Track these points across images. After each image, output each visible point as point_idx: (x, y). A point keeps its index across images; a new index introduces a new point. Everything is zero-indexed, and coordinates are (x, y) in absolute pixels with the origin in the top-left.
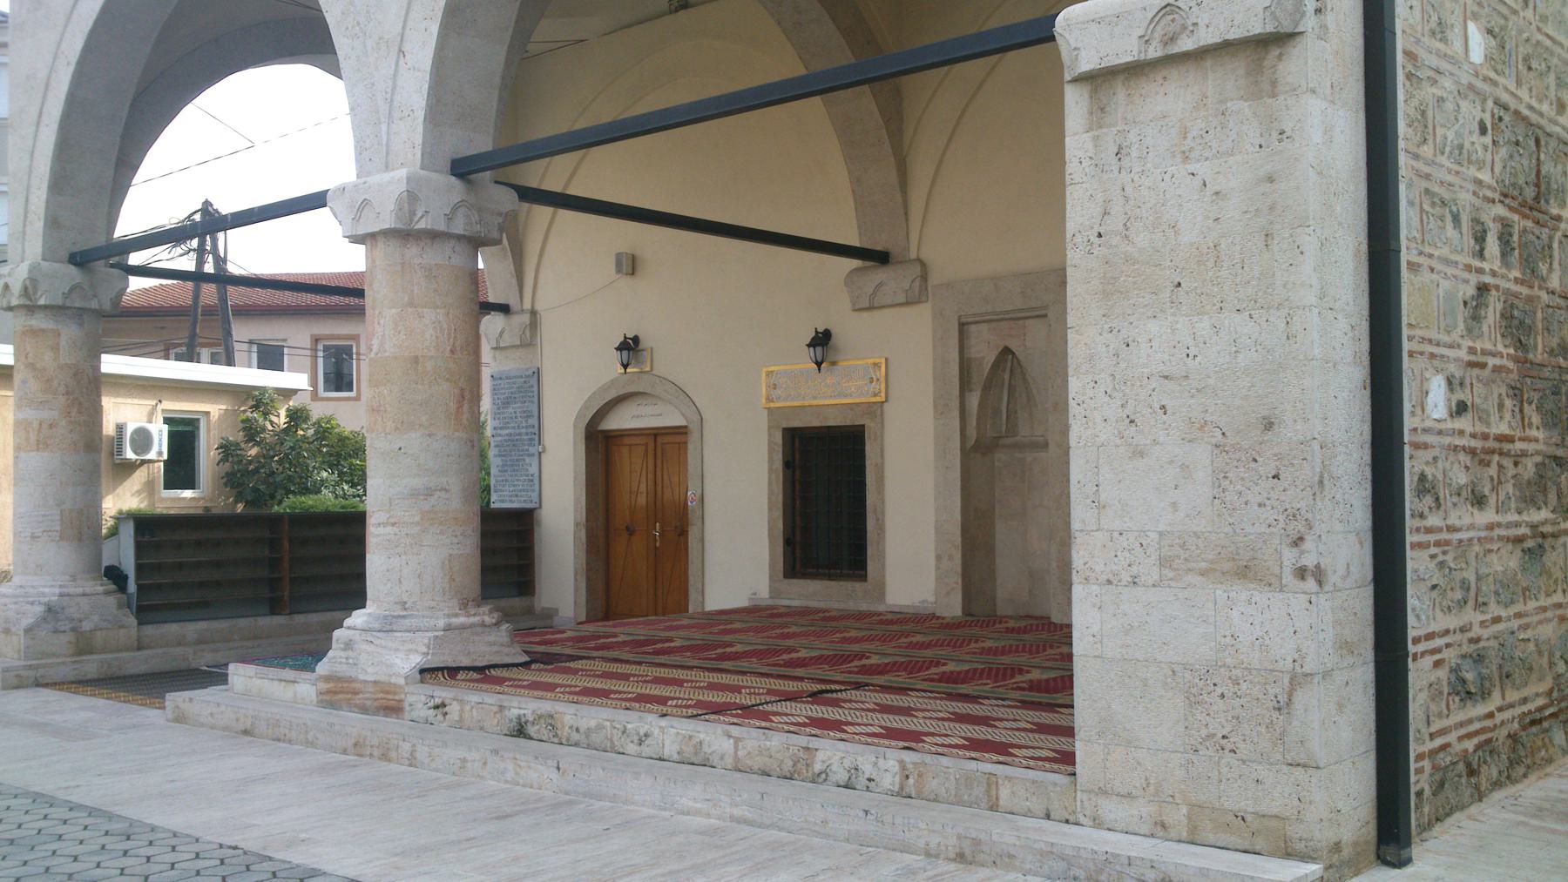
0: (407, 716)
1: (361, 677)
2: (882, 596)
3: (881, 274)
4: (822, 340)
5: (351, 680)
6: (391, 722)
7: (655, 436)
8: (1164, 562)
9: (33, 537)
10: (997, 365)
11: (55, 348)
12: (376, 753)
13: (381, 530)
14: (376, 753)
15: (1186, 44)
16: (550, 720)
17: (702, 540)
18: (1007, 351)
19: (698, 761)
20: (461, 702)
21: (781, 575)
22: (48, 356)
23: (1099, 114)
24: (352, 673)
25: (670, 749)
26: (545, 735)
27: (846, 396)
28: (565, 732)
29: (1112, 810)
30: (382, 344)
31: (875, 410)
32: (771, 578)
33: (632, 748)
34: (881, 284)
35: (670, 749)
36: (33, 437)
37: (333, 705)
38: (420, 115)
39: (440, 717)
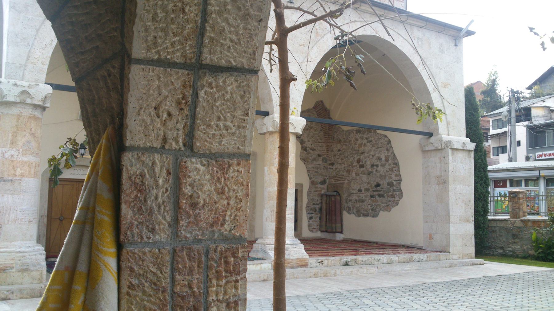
8: (460, 220)
9: (30, 221)
12: (322, 275)
13: (289, 216)
14: (322, 275)
15: (465, 148)
19: (391, 262)
23: (453, 154)
28: (359, 262)
29: (454, 257)
33: (376, 263)
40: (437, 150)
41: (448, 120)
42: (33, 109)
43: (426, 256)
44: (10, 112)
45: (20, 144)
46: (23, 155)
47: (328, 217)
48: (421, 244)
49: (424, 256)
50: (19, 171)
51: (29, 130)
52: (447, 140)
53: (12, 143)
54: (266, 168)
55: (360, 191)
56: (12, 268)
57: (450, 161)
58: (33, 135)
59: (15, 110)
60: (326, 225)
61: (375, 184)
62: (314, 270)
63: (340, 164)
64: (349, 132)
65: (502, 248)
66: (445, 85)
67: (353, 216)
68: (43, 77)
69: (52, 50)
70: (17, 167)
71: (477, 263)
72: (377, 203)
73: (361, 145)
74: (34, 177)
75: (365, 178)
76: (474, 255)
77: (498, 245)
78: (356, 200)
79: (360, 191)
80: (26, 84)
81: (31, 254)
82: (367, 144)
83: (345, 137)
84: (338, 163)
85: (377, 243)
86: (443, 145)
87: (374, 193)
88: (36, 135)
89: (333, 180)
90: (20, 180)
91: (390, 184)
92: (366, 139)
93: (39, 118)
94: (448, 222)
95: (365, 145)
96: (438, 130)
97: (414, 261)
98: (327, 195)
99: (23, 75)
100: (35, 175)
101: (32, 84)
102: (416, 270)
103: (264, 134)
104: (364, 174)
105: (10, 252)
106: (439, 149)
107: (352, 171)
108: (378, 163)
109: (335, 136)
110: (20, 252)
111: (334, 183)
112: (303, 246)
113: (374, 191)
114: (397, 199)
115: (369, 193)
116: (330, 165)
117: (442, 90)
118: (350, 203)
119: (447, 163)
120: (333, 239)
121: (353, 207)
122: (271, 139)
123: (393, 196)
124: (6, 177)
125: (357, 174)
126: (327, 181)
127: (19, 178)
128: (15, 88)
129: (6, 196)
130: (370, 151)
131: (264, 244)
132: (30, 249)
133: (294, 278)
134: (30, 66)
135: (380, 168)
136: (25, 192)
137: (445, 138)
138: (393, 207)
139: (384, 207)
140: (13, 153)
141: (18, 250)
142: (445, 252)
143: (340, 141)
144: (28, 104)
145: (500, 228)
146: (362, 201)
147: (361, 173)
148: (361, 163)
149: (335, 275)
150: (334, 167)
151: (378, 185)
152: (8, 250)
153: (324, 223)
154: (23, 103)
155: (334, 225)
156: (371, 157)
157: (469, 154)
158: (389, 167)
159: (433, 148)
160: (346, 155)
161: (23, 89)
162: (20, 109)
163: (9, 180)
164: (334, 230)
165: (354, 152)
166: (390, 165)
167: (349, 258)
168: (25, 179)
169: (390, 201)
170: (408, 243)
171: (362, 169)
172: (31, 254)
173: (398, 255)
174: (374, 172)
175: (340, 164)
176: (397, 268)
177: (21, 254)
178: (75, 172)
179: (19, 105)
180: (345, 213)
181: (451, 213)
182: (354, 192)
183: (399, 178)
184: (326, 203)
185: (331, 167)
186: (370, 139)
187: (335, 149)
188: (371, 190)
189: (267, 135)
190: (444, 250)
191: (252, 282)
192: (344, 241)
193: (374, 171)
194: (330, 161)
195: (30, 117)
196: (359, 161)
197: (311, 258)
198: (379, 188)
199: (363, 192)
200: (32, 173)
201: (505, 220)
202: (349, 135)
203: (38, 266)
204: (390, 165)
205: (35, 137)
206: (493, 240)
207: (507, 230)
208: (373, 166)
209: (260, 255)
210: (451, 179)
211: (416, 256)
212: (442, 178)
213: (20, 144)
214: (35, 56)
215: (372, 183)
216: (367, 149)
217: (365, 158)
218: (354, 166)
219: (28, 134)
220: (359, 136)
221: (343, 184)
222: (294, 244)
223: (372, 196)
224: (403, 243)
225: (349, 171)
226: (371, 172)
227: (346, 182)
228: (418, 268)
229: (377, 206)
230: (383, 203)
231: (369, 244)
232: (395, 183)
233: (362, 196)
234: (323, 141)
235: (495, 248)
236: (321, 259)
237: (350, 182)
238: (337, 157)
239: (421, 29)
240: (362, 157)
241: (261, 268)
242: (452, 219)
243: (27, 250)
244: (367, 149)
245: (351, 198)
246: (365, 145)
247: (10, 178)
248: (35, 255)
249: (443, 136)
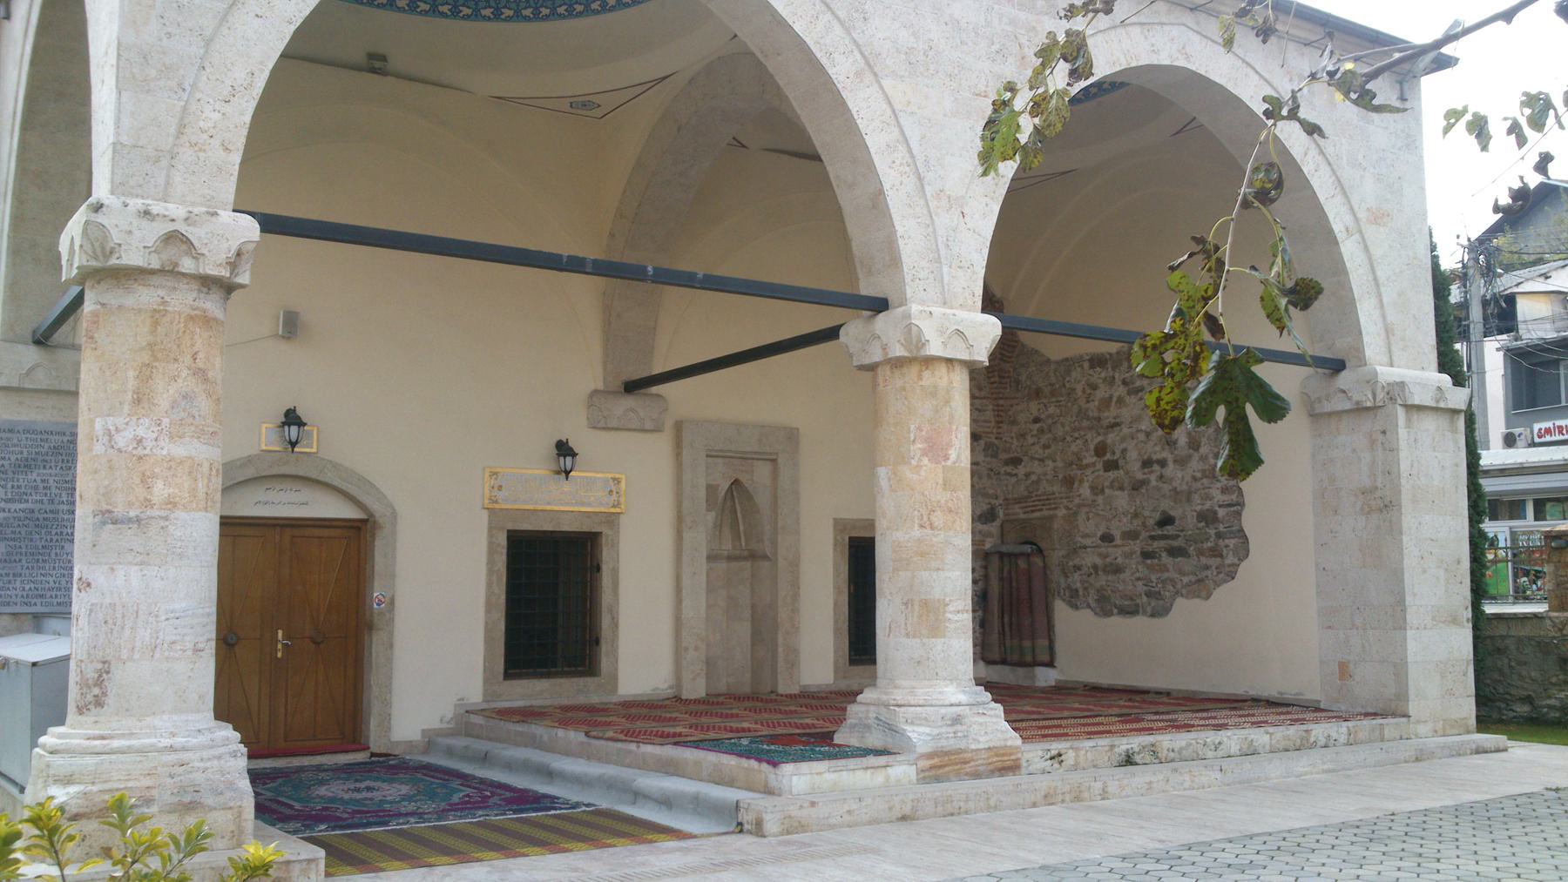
0: (1023, 771)
1: (973, 747)
2: (615, 688)
4: (564, 449)
5: (960, 751)
6: (1008, 781)
7: (282, 526)
8: (1433, 619)
9: (196, 650)
10: (730, 489)
12: (1067, 798)
14: (1067, 798)
15: (1442, 405)
16: (1153, 750)
17: (391, 646)
18: (736, 482)
19: (1251, 752)
20: (1076, 749)
21: (501, 677)
23: (1409, 421)
24: (962, 745)
25: (1234, 749)
26: (1148, 759)
27: (583, 504)
28: (1163, 754)
29: (1422, 729)
30: (958, 457)
31: (612, 519)
32: (486, 681)
33: (1210, 754)
34: (632, 410)
35: (1234, 749)
37: (938, 779)
39: (1056, 765)
40: (1360, 410)
41: (1389, 319)
42: (200, 291)
43: (1344, 730)
44: (130, 301)
45: (163, 402)
46: (171, 438)
47: (1006, 619)
48: (1311, 695)
49: (1339, 730)
50: (160, 490)
51: (188, 360)
52: (1391, 380)
53: (138, 401)
54: (882, 472)
55: (1107, 538)
56: (148, 801)
57: (1403, 444)
58: (201, 374)
59: (146, 296)
60: (1002, 643)
61: (1157, 516)
62: (1043, 784)
63: (1042, 460)
64: (1068, 364)
65: (1528, 700)
66: (1378, 217)
67: (1085, 616)
68: (227, 189)
69: (254, 104)
70: (154, 476)
71: (1488, 745)
72: (1166, 575)
73: (1106, 403)
74: (206, 509)
75: (1122, 500)
76: (1473, 721)
77: (1513, 691)
78: (1095, 567)
79: (1107, 538)
80: (176, 210)
81: (205, 754)
82: (1127, 399)
83: (1053, 380)
84: (1032, 458)
85: (1168, 694)
86: (1381, 395)
87: (1156, 544)
88: (210, 374)
89: (1017, 509)
90: (166, 518)
91: (1208, 517)
92: (1124, 382)
93: (215, 319)
94: (1401, 625)
95: (1120, 401)
96: (1359, 349)
97: (1314, 745)
98: (1002, 555)
99: (168, 184)
101: (196, 210)
102: (1325, 771)
103: (872, 368)
104: (1121, 489)
105: (142, 751)
106: (1368, 409)
107: (1081, 481)
108: (1165, 454)
109: (1023, 378)
110: (172, 749)
111: (1022, 516)
112: (999, 708)
113: (1152, 538)
114: (1230, 559)
115: (1136, 546)
116: (1007, 463)
117: (1370, 231)
118: (1076, 576)
119: (1394, 450)
120: (1027, 683)
121: (1086, 589)
122: (899, 383)
123: (1216, 553)
124: (119, 510)
125: (1096, 490)
126: (1001, 514)
127: (163, 513)
128: (144, 223)
129: (121, 572)
130: (1138, 419)
131: (887, 706)
132: (201, 739)
133: (989, 808)
134: (187, 155)
135: (1171, 469)
136: (181, 556)
137: (1387, 374)
138: (1217, 584)
139: (1188, 585)
140: (141, 432)
141: (166, 742)
142: (1394, 715)
143: (1038, 394)
144: (184, 275)
145: (1520, 640)
146: (1118, 570)
147: (1111, 487)
148: (1108, 456)
149: (1104, 795)
150: (1021, 470)
151: (1166, 521)
152: (134, 742)
153: (995, 636)
154: (170, 272)
155: (1027, 644)
156: (1141, 436)
157: (1452, 421)
158: (1201, 466)
159: (1347, 406)
160: (1060, 432)
161: (171, 227)
162: (161, 292)
163: (130, 520)
164: (1029, 658)
165: (1085, 423)
166: (1203, 459)
167: (1134, 742)
168: (180, 514)
169: (1207, 567)
170: (1270, 691)
171: (1112, 474)
172: (205, 754)
173: (1271, 729)
174: (1154, 483)
175: (1042, 460)
176: (1274, 769)
177: (173, 757)
178: (272, 496)
179: (155, 280)
180: (1061, 609)
181: (1409, 599)
182: (1087, 542)
183: (1234, 497)
184: (1001, 579)
185: (1009, 469)
186: (1138, 383)
187: (1021, 418)
188: (1144, 535)
189: (884, 372)
190: (1390, 708)
191: (870, 823)
192: (1062, 690)
193: (1153, 478)
194: (1007, 450)
195: (191, 318)
196: (1100, 450)
197: (1028, 747)
198: (1169, 530)
199: (1118, 541)
200: (201, 495)
201: (1535, 616)
202: (1068, 372)
203: (228, 795)
204: (1203, 459)
205: (206, 380)
206: (1496, 676)
207: (1543, 647)
208: (1147, 463)
209: (874, 740)
210: (1405, 499)
211: (1320, 731)
212: (1379, 493)
213: (163, 402)
214: (201, 124)
215: (1146, 513)
216: (1126, 414)
217: (1123, 439)
218: (1088, 466)
219: (185, 373)
220: (1099, 375)
221: (1051, 518)
222: (978, 704)
223: (1146, 555)
224: (1253, 693)
225: (1069, 482)
226: (1143, 483)
227: (1061, 512)
228: (1330, 766)
229: (1164, 582)
230: (1183, 573)
231: (1146, 697)
232: (1221, 513)
233: (1116, 554)
234: (983, 394)
235: (1505, 701)
236: (1056, 746)
237: (1076, 514)
238: (1030, 440)
239: (1307, 50)
240: (1111, 438)
241: (887, 778)
242: (1412, 617)
243: (194, 741)
244: (1126, 414)
245: (1077, 561)
246: (1120, 401)
247: (132, 514)
248: (220, 758)
249: (1378, 368)
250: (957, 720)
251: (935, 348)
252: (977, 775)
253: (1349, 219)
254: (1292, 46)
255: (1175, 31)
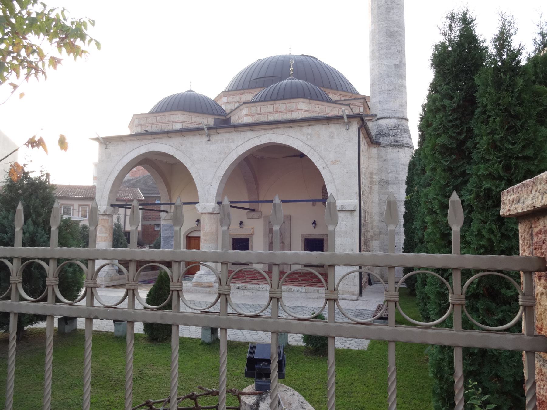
3: (253, 213)
4: (241, 223)
11: (108, 222)
16: (245, 287)
22: (107, 224)
31: (251, 236)
36: (103, 239)
37: (196, 287)
38: (215, 195)
58: (103, 226)
66: (334, 163)
100: (105, 241)
167: (240, 285)
250: (200, 277)
251: (200, 211)
252: (204, 287)
253: (324, 165)
254: (304, 127)
255: (267, 135)
